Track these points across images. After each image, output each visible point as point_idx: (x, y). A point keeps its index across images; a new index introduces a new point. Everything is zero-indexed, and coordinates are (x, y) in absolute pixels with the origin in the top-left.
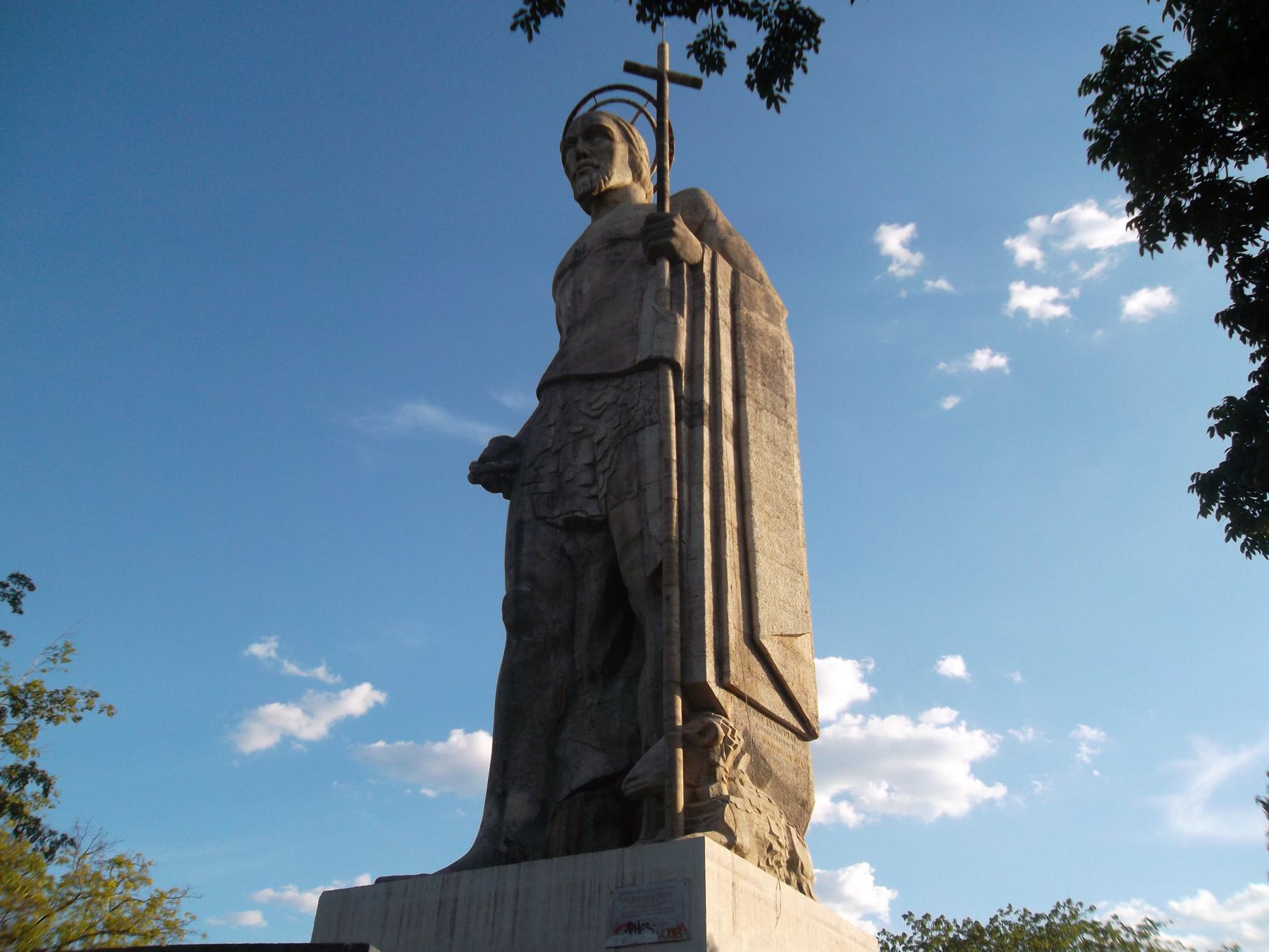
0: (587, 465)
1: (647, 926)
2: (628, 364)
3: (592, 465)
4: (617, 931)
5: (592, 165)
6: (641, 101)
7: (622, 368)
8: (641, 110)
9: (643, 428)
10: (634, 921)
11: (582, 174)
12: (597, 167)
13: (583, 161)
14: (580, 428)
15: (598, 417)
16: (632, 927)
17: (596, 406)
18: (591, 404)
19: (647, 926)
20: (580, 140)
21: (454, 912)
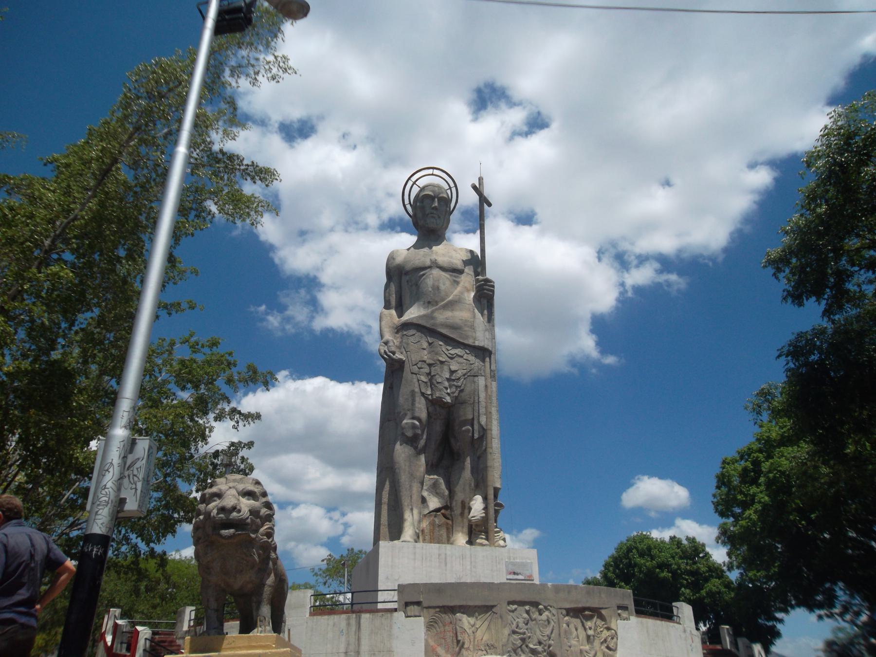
0: (447, 378)
1: (520, 574)
2: (470, 342)
3: (448, 380)
4: (510, 574)
5: (438, 215)
6: (452, 185)
7: (466, 342)
8: (450, 188)
9: (477, 376)
10: (516, 571)
11: (433, 217)
12: (439, 217)
13: (435, 212)
14: (444, 360)
15: (452, 358)
16: (514, 573)
17: (449, 352)
18: (448, 350)
19: (520, 574)
20: (436, 200)
21: (446, 558)
